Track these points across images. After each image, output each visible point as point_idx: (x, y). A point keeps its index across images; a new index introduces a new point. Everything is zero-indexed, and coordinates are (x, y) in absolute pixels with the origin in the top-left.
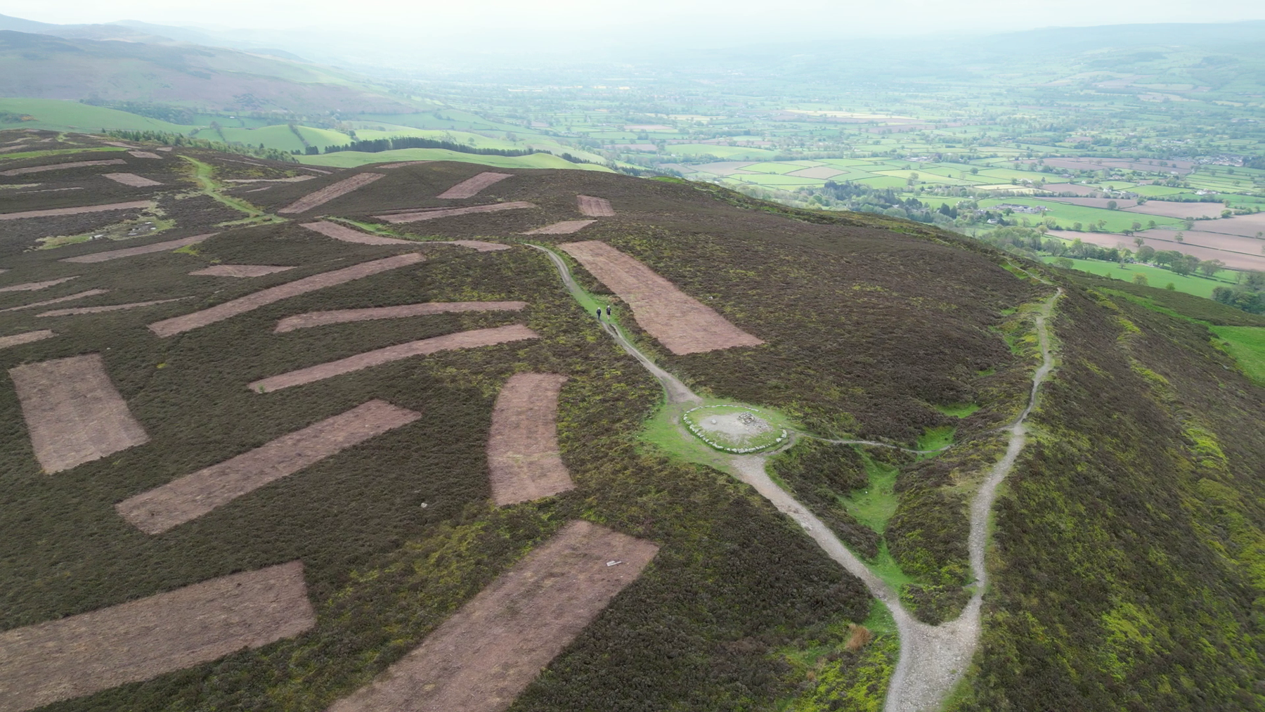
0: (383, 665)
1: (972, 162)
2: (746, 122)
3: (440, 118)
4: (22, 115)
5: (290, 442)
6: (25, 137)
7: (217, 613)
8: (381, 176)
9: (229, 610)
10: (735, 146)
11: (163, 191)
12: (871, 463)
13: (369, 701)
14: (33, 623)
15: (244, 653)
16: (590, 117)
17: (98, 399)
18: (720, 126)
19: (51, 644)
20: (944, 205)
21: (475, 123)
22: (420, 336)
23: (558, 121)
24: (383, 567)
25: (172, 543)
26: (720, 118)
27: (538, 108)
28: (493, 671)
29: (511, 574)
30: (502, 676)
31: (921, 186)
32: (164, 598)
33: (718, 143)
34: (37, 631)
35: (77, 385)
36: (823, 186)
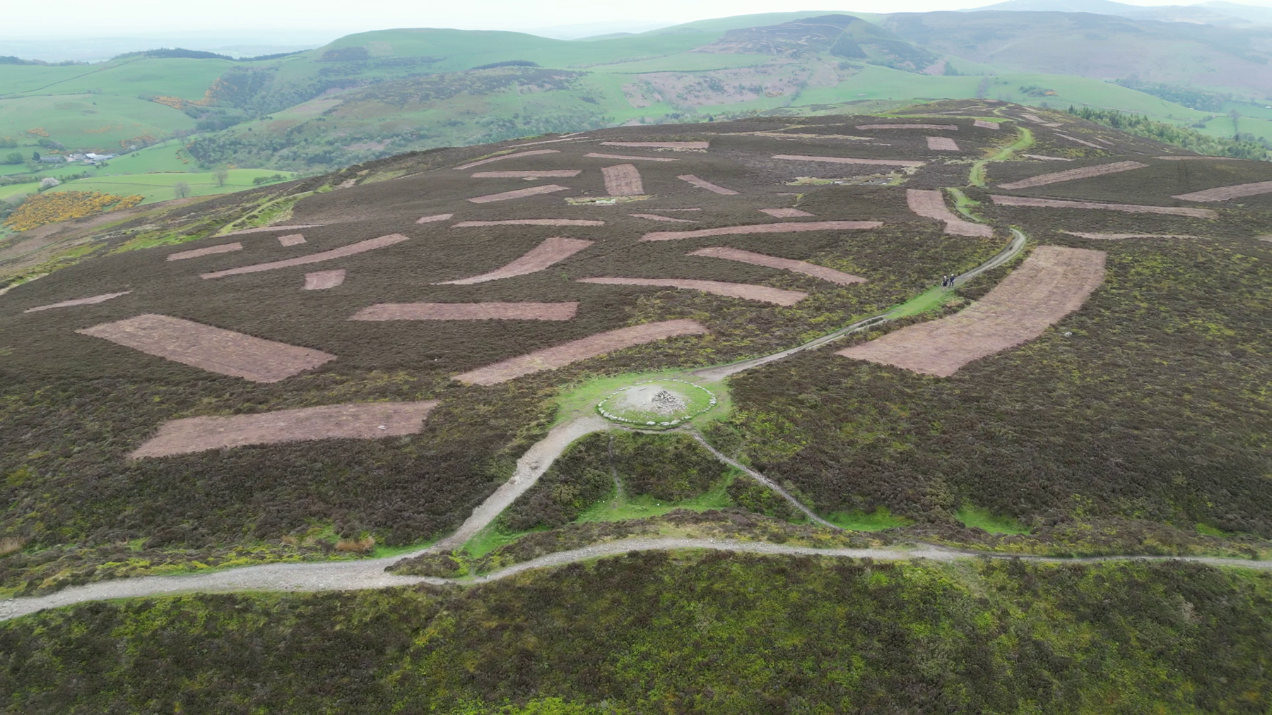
4: (1047, 90)
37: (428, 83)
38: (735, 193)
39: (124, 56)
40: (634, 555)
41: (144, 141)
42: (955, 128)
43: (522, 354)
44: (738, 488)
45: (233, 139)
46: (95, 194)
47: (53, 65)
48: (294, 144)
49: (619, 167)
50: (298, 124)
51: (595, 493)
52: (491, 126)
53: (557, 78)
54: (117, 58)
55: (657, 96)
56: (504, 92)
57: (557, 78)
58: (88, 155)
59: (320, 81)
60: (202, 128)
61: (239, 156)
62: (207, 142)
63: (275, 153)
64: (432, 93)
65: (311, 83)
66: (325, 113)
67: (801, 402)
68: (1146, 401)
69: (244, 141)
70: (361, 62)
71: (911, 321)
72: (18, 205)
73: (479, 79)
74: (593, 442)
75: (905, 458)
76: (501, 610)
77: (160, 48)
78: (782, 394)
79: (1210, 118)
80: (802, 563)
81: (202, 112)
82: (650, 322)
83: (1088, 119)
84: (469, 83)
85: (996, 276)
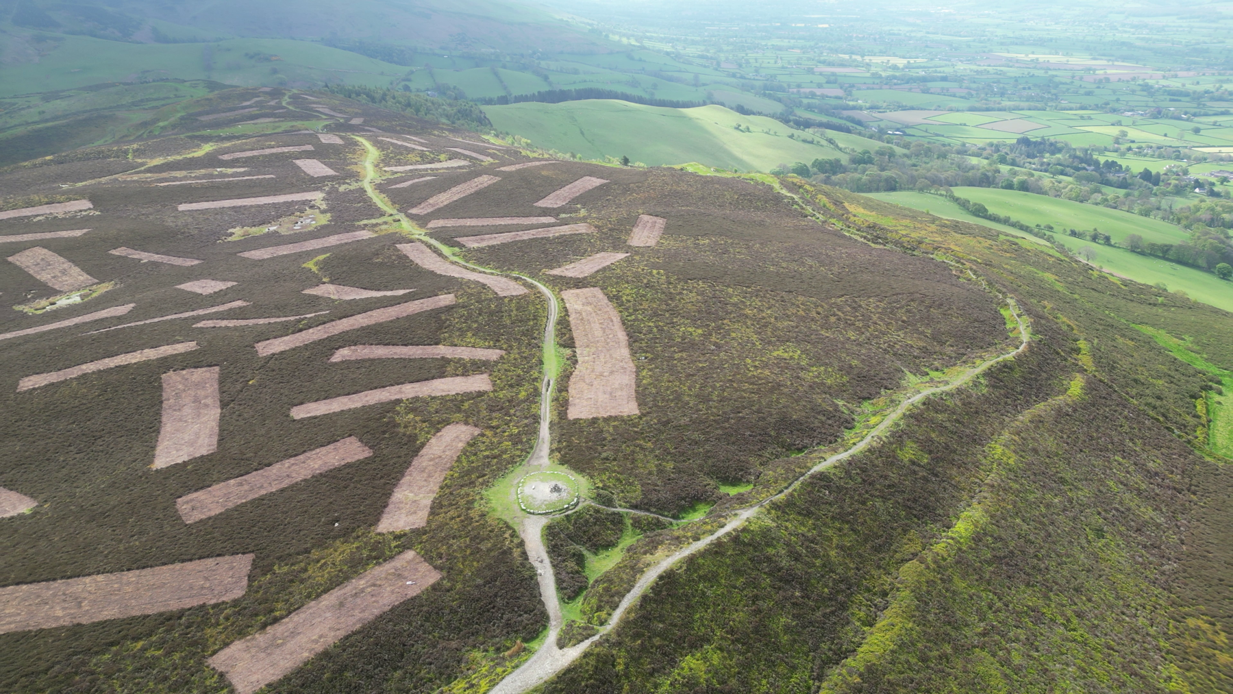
0: (264, 626)
1: (1196, 119)
2: (946, 66)
3: (632, 59)
5: (287, 465)
6: (259, 96)
7: (200, 579)
8: (498, 179)
9: (206, 579)
10: (928, 93)
11: (332, 181)
12: (630, 526)
13: (249, 644)
14: (111, 572)
15: (204, 606)
16: (781, 58)
17: (206, 406)
18: (917, 70)
19: (116, 586)
20: (1146, 169)
21: (665, 64)
22: (411, 380)
23: (748, 62)
24: (293, 564)
25: (195, 531)
26: (918, 60)
27: (730, 48)
28: (314, 638)
29: (354, 581)
30: (316, 641)
31: (1128, 145)
32: (178, 566)
33: (910, 90)
34: (112, 577)
35: (199, 392)
36: (1015, 141)
38: (196, 262)
40: (661, 577)
42: (309, 148)
43: (390, 494)
44: (637, 523)
51: (580, 559)
67: (607, 459)
68: (725, 394)
71: (565, 379)
74: (551, 533)
75: (678, 470)
76: (637, 636)
78: (594, 458)
79: (412, 72)
80: (719, 544)
83: (350, 97)
85: (564, 325)
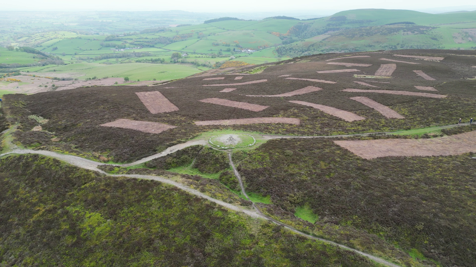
37: (365, 30)
39: (267, 18)
41: (265, 47)
45: (290, 47)
46: (243, 63)
47: (246, 21)
48: (310, 50)
49: (389, 65)
50: (313, 43)
52: (386, 47)
53: (421, 29)
54: (265, 19)
55: (470, 39)
56: (395, 34)
57: (421, 29)
58: (248, 50)
59: (326, 28)
60: (284, 43)
61: (291, 53)
62: (282, 48)
63: (303, 53)
64: (365, 34)
65: (323, 28)
66: (323, 40)
69: (294, 48)
70: (343, 21)
72: (223, 64)
73: (386, 29)
77: (278, 16)
81: (285, 38)
82: (282, 117)
84: (381, 30)
